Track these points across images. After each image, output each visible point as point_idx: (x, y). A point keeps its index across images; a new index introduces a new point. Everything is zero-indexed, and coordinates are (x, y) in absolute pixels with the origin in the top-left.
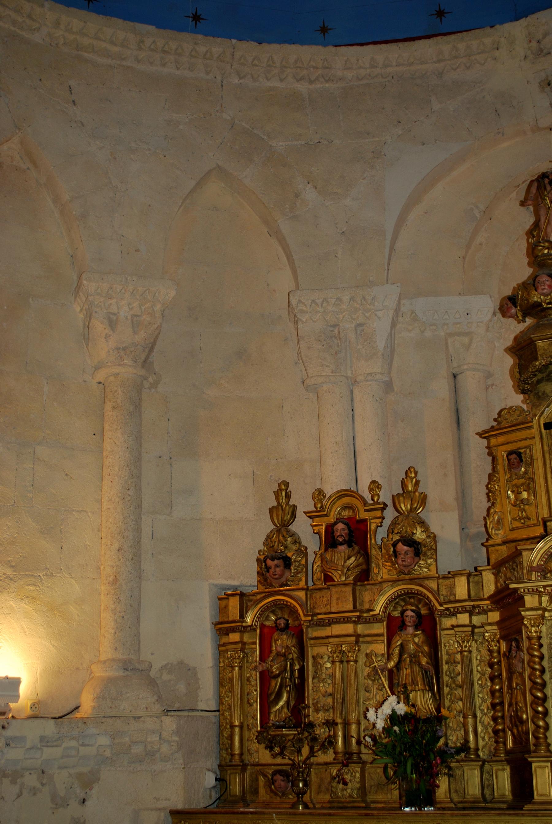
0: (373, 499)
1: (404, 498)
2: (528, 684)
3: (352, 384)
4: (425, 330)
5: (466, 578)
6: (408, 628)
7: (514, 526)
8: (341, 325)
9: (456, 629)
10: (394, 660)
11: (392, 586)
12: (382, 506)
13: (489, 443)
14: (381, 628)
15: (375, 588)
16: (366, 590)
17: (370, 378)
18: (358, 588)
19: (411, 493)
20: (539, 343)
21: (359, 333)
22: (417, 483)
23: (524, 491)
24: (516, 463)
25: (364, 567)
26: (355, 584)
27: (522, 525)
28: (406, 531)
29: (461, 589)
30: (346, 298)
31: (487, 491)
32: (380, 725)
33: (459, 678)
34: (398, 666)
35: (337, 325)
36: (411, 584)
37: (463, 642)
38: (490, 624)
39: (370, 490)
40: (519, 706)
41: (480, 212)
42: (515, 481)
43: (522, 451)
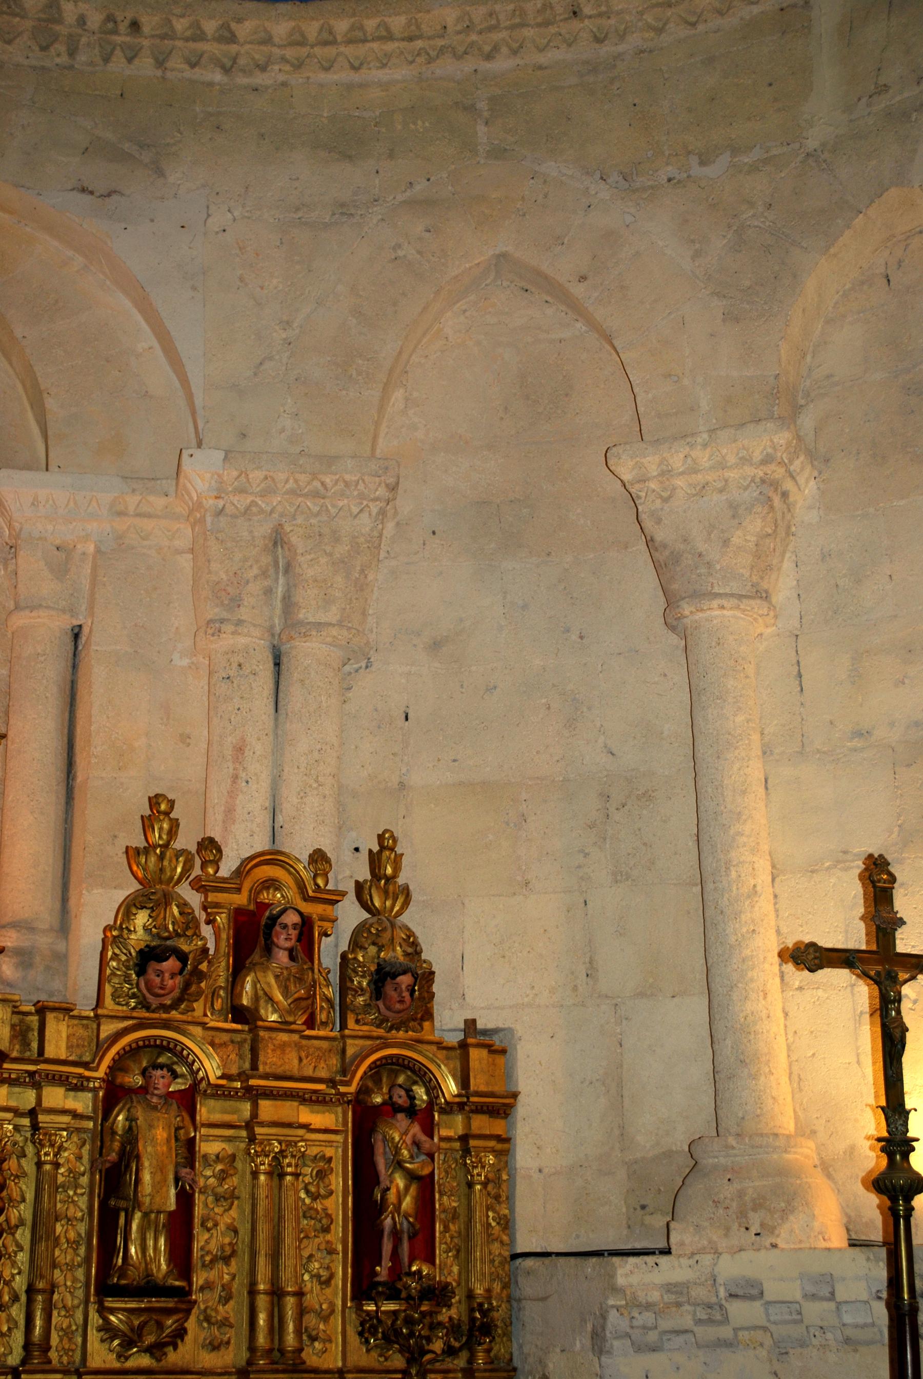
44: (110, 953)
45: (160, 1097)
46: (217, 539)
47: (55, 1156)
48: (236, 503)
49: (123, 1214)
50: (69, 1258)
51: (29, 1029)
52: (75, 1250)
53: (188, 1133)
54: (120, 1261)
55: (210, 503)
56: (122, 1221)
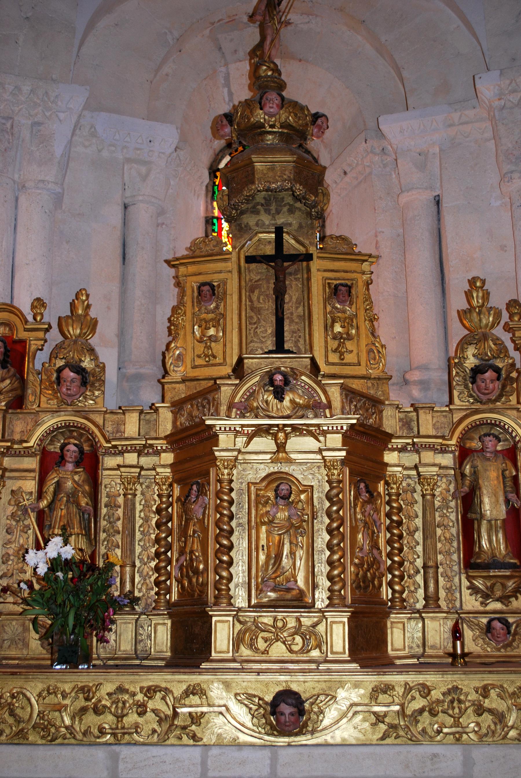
0: (35, 319)
1: (73, 320)
2: (213, 530)
3: (18, 189)
4: (102, 149)
5: (138, 414)
6: (67, 463)
7: (196, 364)
8: (16, 118)
9: (122, 469)
10: (47, 499)
11: (53, 417)
12: (47, 326)
13: (177, 272)
14: (32, 463)
15: (29, 418)
16: (19, 419)
17: (41, 185)
18: (8, 416)
19: (80, 316)
20: (258, 166)
21: (34, 132)
22: (88, 306)
23: (213, 326)
24: (208, 296)
25: (19, 392)
26: (6, 412)
27: (205, 363)
28: (73, 358)
29: (132, 426)
30: (26, 89)
31: (169, 325)
32: (42, 570)
33: (119, 524)
34: (50, 506)
35: (11, 118)
36: (75, 416)
37: (129, 484)
38: (164, 466)
39: (33, 307)
40: (195, 555)
41: (173, 39)
42: (203, 316)
43: (215, 284)
44: (454, 373)
45: (491, 453)
46: (503, 124)
47: (432, 490)
48: (511, 100)
49: (476, 522)
50: (447, 548)
51: (411, 420)
52: (451, 544)
53: (511, 473)
54: (477, 550)
55: (496, 103)
56: (476, 526)
